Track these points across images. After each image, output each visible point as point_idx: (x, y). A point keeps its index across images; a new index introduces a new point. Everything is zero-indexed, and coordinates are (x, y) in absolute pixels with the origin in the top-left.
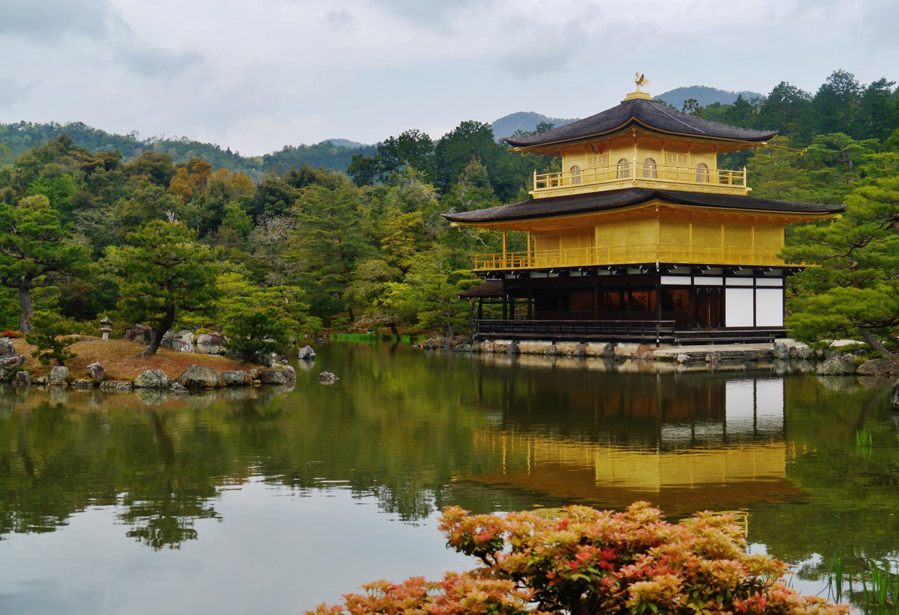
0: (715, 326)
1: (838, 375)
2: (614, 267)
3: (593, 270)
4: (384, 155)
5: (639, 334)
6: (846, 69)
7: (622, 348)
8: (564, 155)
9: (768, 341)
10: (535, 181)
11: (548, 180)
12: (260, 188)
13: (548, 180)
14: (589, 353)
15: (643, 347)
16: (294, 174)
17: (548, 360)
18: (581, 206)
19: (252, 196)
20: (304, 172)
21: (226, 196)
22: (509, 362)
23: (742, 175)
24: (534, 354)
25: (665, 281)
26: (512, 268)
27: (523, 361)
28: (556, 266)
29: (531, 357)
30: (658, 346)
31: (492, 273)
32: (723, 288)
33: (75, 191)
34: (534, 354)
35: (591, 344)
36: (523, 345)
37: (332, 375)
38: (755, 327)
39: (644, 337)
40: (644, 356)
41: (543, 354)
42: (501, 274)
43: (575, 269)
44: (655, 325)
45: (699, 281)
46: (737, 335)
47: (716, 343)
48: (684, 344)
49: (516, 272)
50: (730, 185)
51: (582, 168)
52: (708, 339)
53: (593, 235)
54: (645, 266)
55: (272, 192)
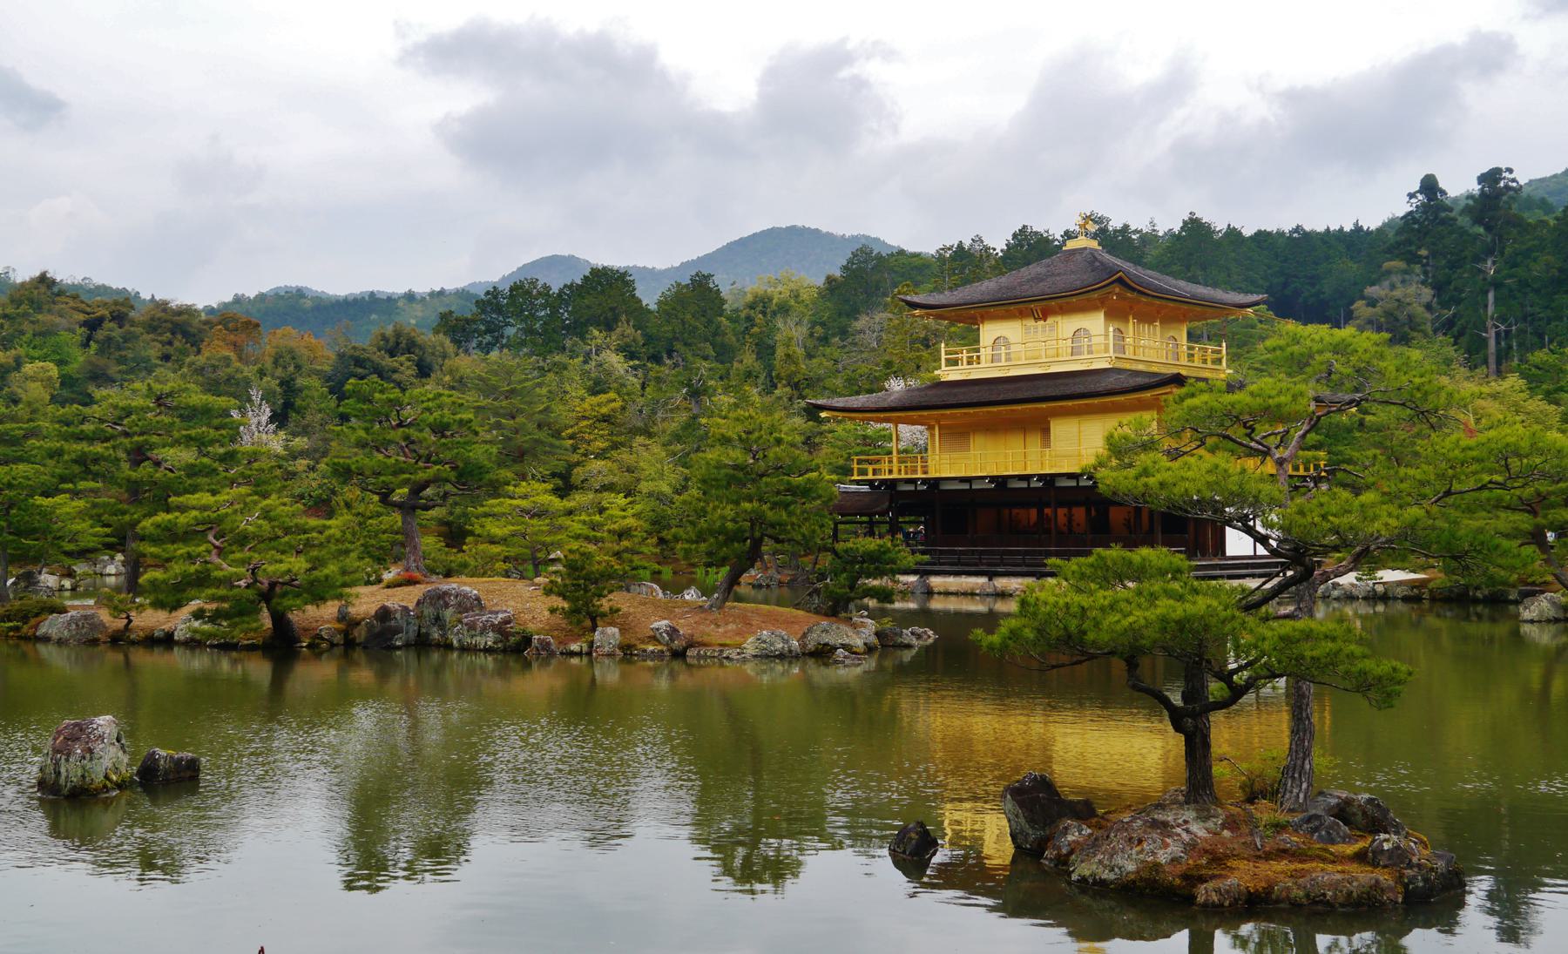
0: (1215, 555)
1: (1549, 621)
3: (1049, 479)
4: (484, 311)
6: (1101, 212)
10: (943, 356)
11: (965, 355)
12: (341, 356)
16: (384, 338)
17: (983, 603)
18: (1042, 393)
19: (327, 368)
20: (398, 334)
21: (298, 367)
22: (912, 606)
23: (1219, 352)
24: (956, 594)
26: (920, 475)
27: (936, 604)
29: (953, 598)
31: (883, 482)
33: (79, 360)
34: (956, 594)
36: (935, 581)
37: (931, 633)
38: (1255, 556)
41: (973, 594)
42: (891, 484)
43: (1027, 478)
46: (1247, 566)
47: (1231, 577)
49: (924, 481)
50: (1209, 365)
51: (1012, 340)
52: (1218, 572)
53: (1046, 431)
55: (359, 362)
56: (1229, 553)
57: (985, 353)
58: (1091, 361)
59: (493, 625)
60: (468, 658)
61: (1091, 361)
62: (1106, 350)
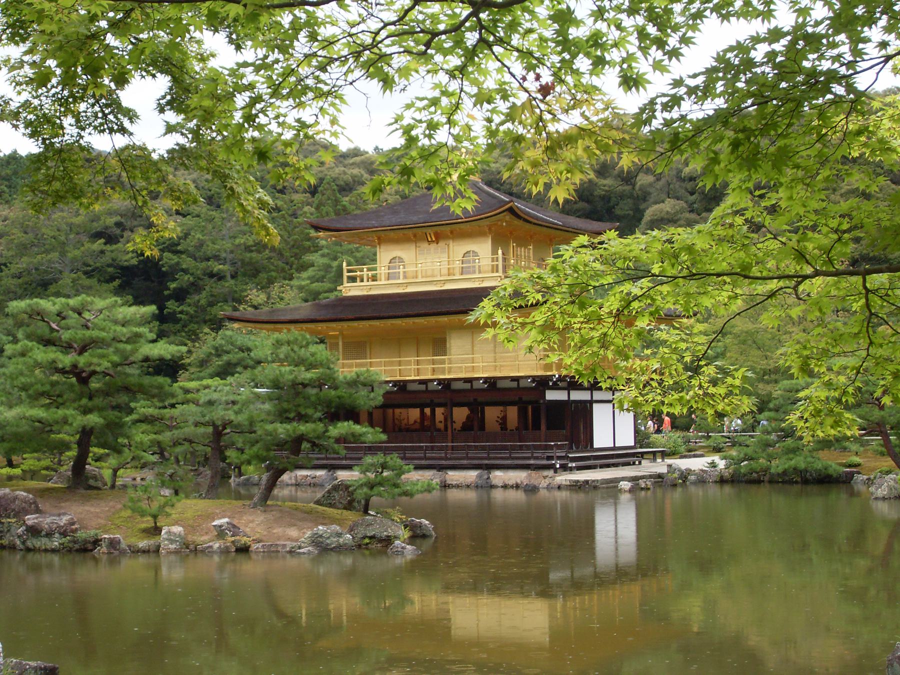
2: (486, 380)
3: (446, 384)
5: (529, 458)
7: (498, 476)
8: (379, 244)
9: (634, 464)
10: (346, 274)
11: (365, 273)
13: (365, 273)
14: (449, 482)
15: (533, 473)
25: (551, 395)
28: (398, 378)
30: (556, 472)
32: (591, 402)
35: (451, 473)
38: (614, 448)
39: (532, 462)
40: (544, 483)
44: (551, 447)
45: (576, 396)
47: (602, 466)
48: (579, 468)
54: (534, 378)
56: (596, 445)
57: (382, 269)
58: (483, 279)
59: (59, 527)
60: (30, 556)
61: (483, 279)
62: (497, 271)
